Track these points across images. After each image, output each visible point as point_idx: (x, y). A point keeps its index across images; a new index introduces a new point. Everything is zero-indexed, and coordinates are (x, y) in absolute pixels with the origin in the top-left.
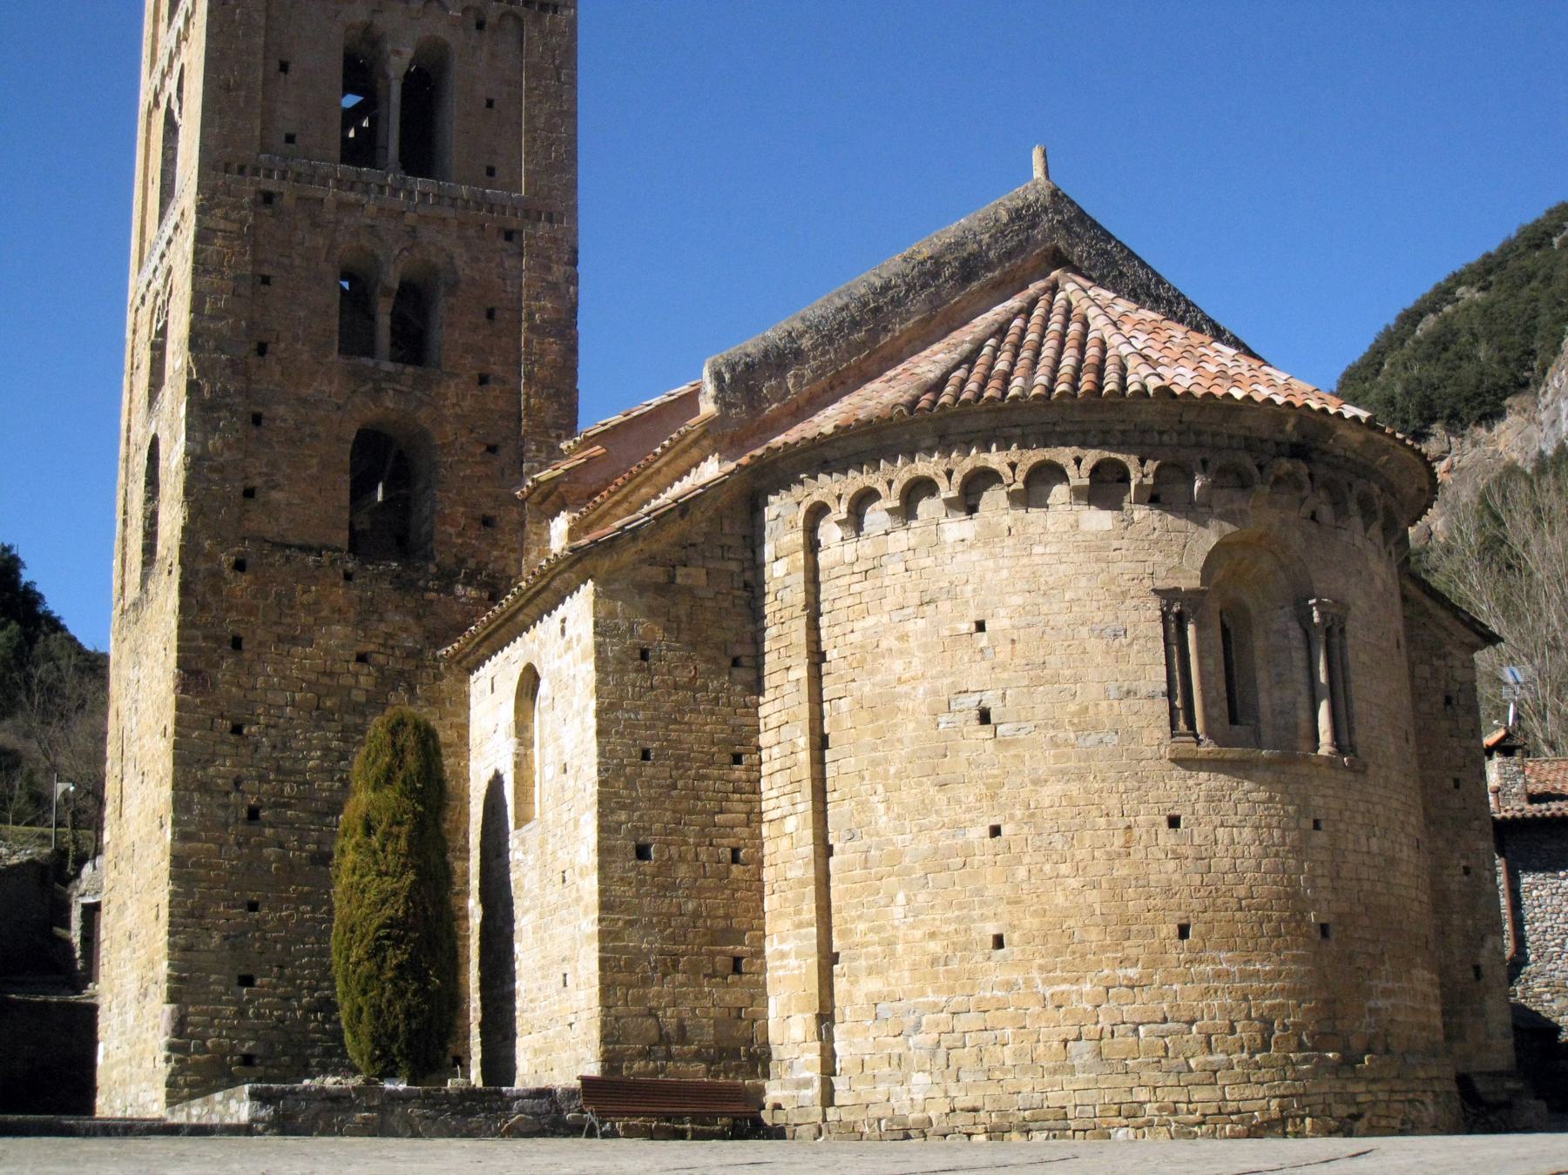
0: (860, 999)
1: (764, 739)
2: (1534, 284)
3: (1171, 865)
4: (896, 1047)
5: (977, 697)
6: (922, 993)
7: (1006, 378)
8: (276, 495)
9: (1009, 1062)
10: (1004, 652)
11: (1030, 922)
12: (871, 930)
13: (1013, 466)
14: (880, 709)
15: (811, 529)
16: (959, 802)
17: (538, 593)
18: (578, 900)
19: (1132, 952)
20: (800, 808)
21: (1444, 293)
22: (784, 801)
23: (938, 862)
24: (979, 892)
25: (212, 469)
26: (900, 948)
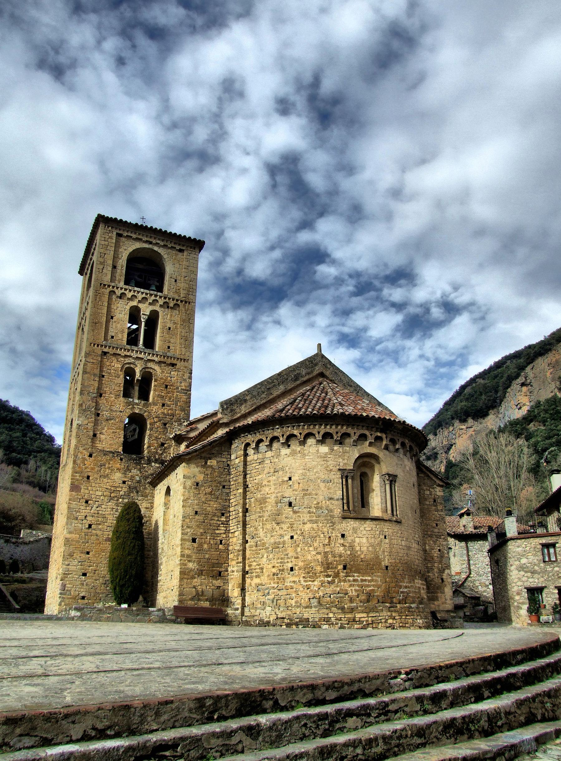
0: (253, 585)
1: (231, 509)
2: (498, 378)
3: (342, 548)
4: (262, 599)
5: (289, 499)
6: (270, 584)
7: (300, 409)
8: (103, 437)
9: (294, 604)
10: (296, 486)
11: (301, 564)
12: (257, 565)
13: (300, 434)
14: (263, 501)
15: (245, 450)
16: (282, 528)
17: (170, 466)
18: (176, 554)
19: (330, 573)
20: (239, 529)
22: (235, 527)
23: (276, 546)
24: (287, 555)
25: (84, 429)
26: (264, 570)
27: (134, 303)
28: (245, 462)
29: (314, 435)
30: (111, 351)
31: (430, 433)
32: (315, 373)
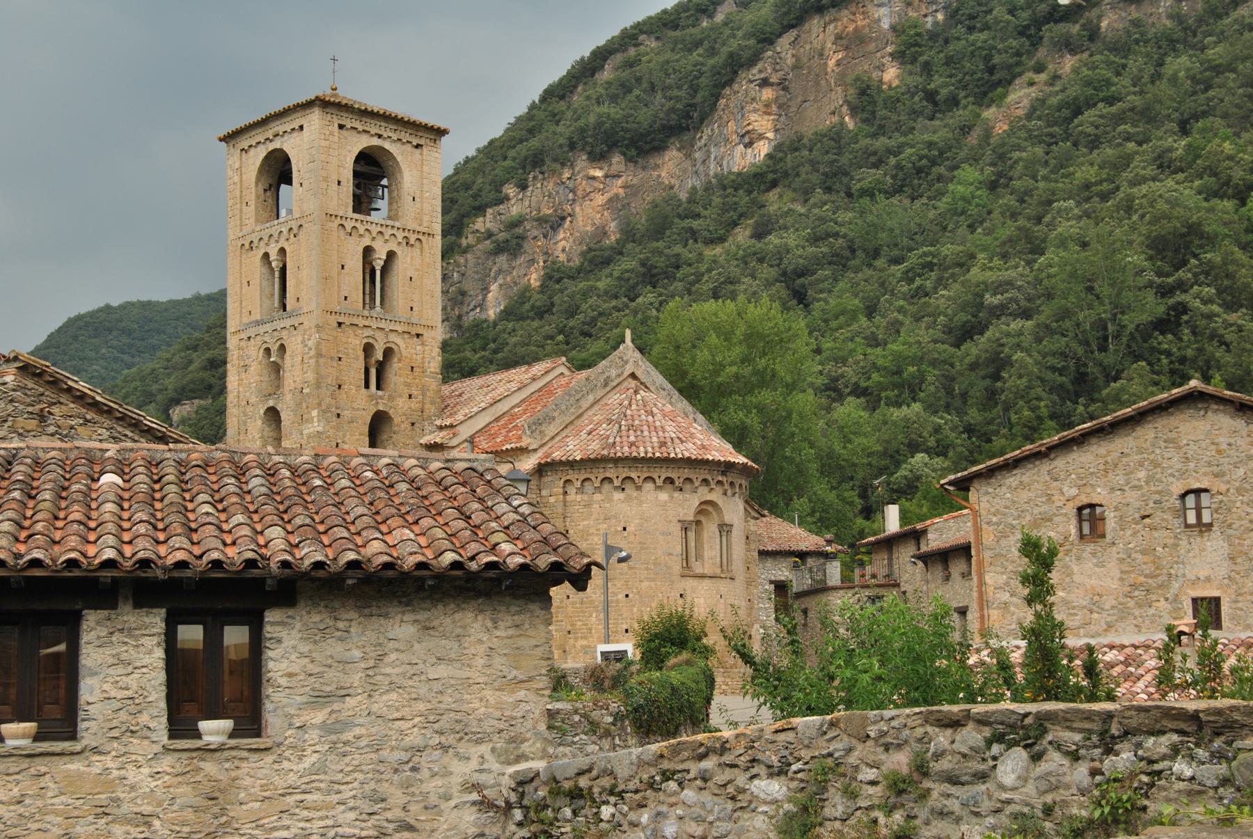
2: (700, 51)
10: (632, 538)
21: (630, 37)
27: (366, 241)
28: (565, 501)
29: (654, 480)
30: (347, 320)
31: (507, 181)
32: (626, 374)
